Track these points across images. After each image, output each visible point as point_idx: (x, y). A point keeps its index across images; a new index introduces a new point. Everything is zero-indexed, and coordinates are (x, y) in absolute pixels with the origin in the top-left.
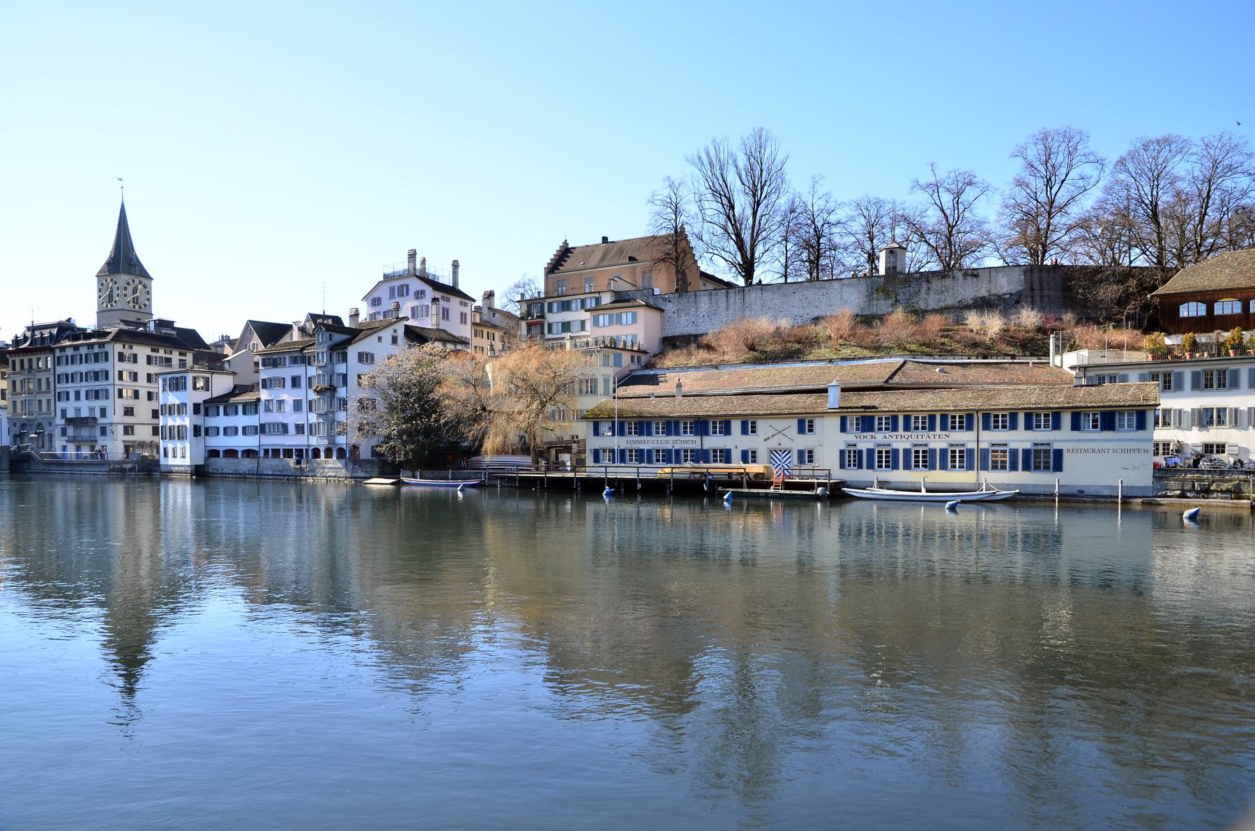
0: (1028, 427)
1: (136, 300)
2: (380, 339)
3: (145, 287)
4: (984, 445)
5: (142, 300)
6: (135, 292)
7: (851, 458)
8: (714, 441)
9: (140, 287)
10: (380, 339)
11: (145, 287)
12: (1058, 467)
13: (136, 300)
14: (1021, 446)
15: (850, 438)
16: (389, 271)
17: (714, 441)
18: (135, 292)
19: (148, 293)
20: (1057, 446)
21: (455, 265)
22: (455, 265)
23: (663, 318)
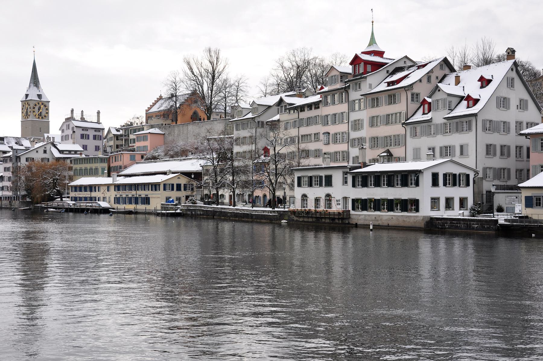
0: (144, 190)
1: (40, 114)
2: (37, 152)
3: (45, 106)
4: (137, 196)
5: (44, 114)
6: (39, 109)
7: (117, 200)
8: (94, 194)
9: (42, 106)
10: (37, 152)
11: (45, 106)
12: (149, 204)
13: (40, 114)
14: (143, 196)
15: (116, 193)
16: (66, 117)
17: (94, 194)
18: (39, 109)
19: (47, 109)
20: (149, 196)
21: (99, 113)
22: (99, 113)
23: (164, 137)
